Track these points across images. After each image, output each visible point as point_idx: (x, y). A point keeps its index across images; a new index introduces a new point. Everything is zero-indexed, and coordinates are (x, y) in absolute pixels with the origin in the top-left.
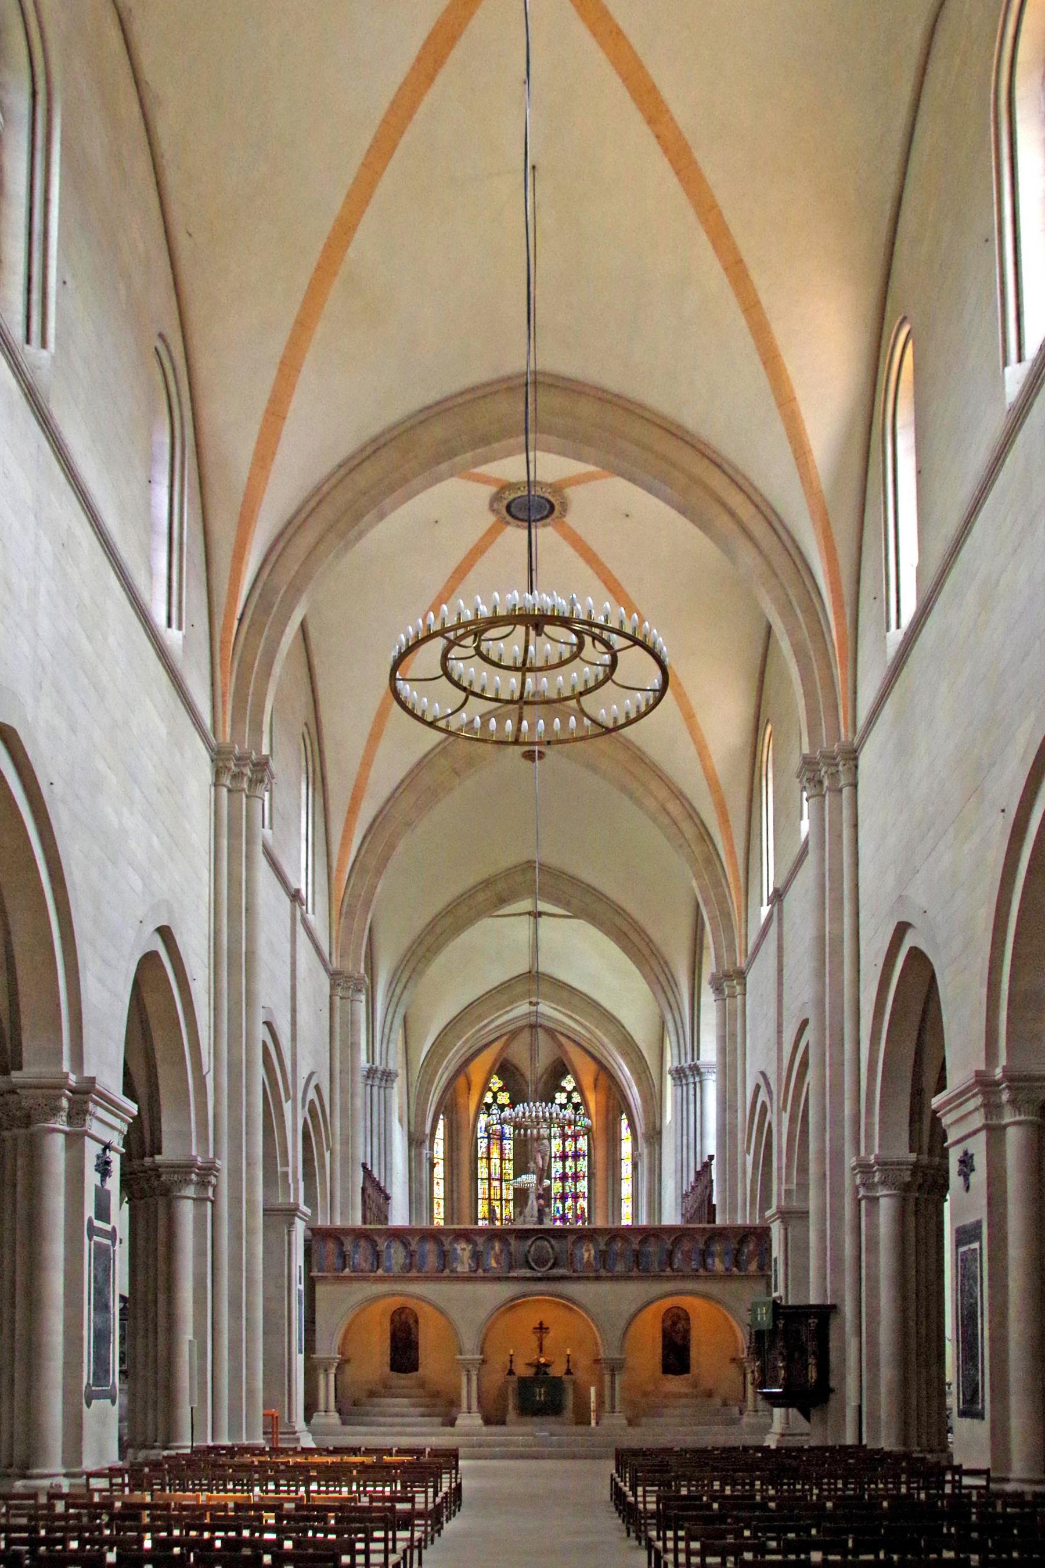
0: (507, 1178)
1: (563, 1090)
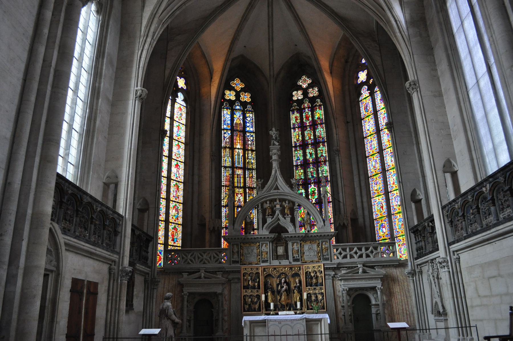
0: (250, 167)
1: (300, 88)
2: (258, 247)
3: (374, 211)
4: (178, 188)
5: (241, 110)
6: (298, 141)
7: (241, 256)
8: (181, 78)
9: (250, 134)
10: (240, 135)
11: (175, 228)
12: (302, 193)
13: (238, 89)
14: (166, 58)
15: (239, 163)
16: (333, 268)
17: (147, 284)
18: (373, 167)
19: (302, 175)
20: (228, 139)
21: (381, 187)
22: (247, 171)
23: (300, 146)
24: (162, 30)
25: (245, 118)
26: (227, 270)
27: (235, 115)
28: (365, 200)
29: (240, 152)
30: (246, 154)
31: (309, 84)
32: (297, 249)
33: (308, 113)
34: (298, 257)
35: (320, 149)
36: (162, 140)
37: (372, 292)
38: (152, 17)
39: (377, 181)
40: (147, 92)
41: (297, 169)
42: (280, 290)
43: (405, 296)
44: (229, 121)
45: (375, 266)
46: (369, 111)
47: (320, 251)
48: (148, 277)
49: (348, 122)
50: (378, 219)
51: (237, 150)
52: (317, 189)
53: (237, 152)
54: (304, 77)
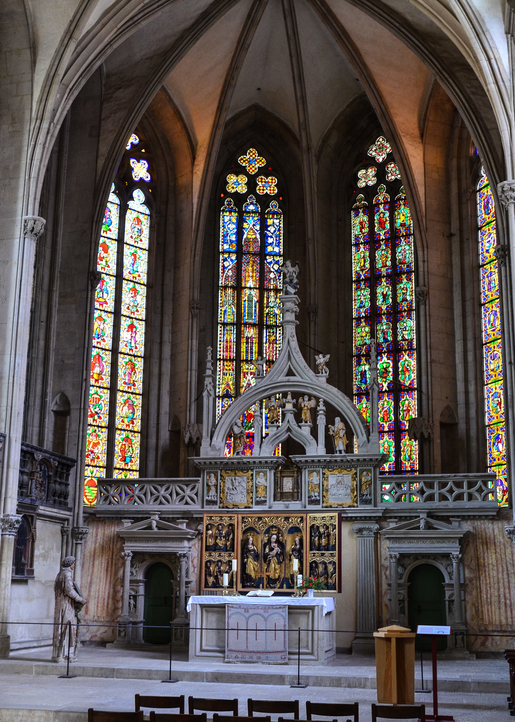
2: (251, 478)
3: (486, 409)
4: (133, 369)
5: (258, 212)
6: (362, 270)
7: (220, 492)
8: (139, 162)
9: (274, 260)
10: (254, 262)
11: (127, 439)
12: (365, 371)
13: (253, 171)
14: (99, 136)
15: (250, 314)
16: (377, 518)
17: (65, 537)
18: (490, 326)
19: (367, 337)
20: (230, 271)
21: (500, 365)
22: (265, 330)
23: (366, 280)
24: (71, 102)
25: (264, 227)
26: (194, 516)
27: (245, 224)
28: (472, 388)
29: (254, 295)
30: (265, 299)
31: (388, 155)
32: (316, 483)
33: (384, 214)
34: (319, 496)
35: (402, 287)
36: (91, 290)
37: (445, 562)
38: (49, 83)
39: (496, 352)
40: (44, 221)
41: (358, 326)
42: (268, 554)
43: (505, 572)
44: (234, 236)
45: (453, 517)
46: (491, 214)
47: (357, 488)
48: (68, 525)
49: (451, 235)
50: (492, 425)
51: (247, 291)
52: (392, 365)
53: (247, 294)
54: (381, 140)
